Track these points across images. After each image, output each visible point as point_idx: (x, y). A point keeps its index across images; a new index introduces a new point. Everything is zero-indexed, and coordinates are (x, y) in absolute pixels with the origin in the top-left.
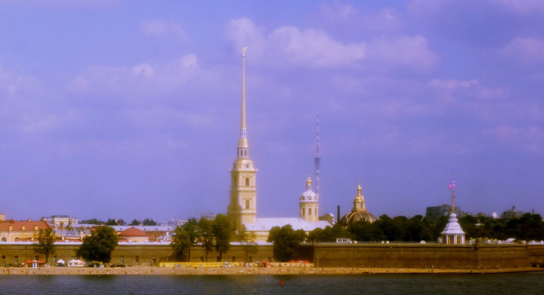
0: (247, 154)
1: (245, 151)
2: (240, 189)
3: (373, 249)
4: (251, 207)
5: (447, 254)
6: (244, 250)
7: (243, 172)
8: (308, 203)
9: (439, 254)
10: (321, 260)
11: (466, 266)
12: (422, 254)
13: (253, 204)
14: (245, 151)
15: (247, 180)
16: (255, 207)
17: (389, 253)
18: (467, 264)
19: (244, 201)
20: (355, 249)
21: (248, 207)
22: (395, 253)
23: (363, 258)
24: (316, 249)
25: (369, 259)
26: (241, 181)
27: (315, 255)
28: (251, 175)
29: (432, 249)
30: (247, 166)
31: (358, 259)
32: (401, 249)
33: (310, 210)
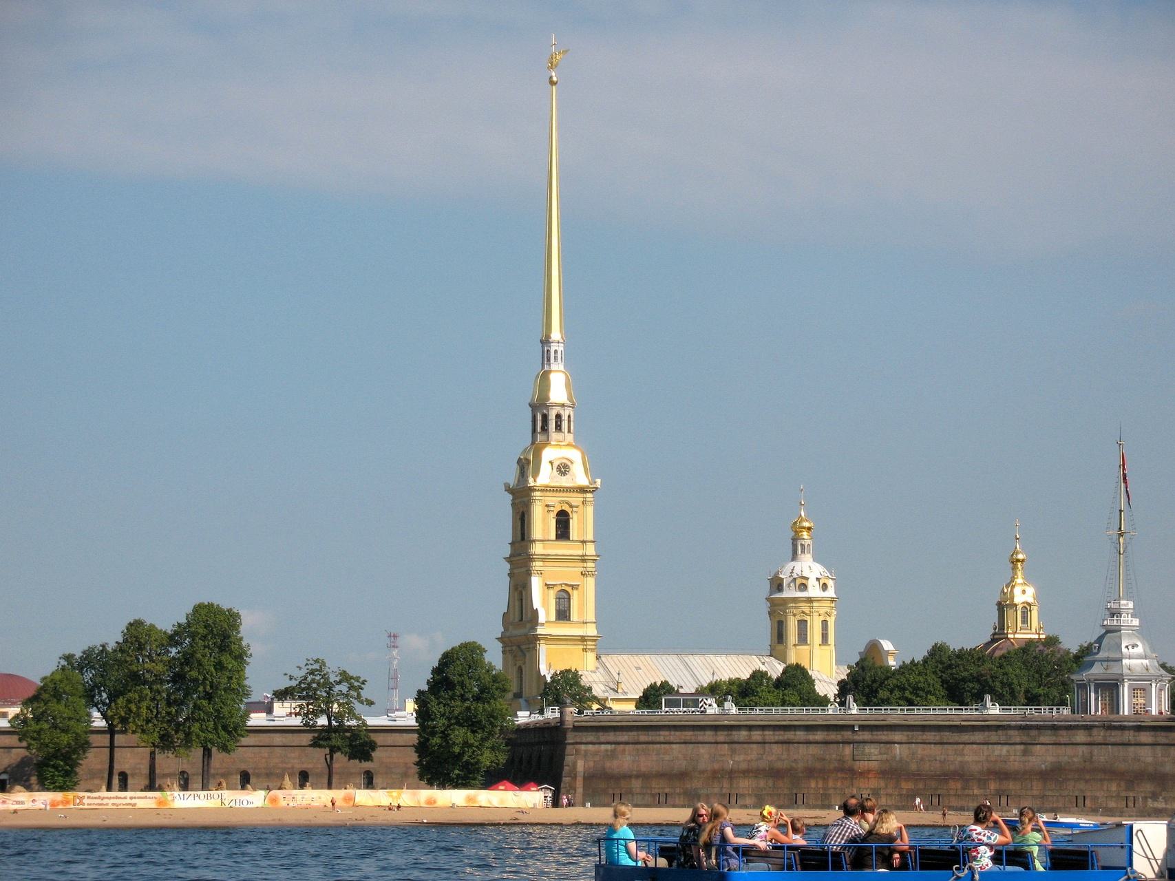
0: (565, 425)
1: (558, 416)
2: (537, 549)
3: (790, 735)
4: (574, 616)
5: (1073, 756)
6: (315, 744)
7: (546, 489)
8: (795, 600)
9: (1043, 756)
10: (589, 778)
11: (1150, 803)
12: (973, 756)
13: (585, 604)
14: (558, 416)
15: (563, 522)
16: (591, 617)
17: (848, 750)
18: (1154, 797)
19: (552, 594)
20: (722, 736)
21: (563, 614)
22: (872, 750)
23: (746, 773)
24: (571, 737)
25: (775, 774)
26: (542, 524)
27: (569, 759)
28: (576, 499)
29: (1016, 736)
30: (563, 469)
31: (731, 774)
32: (897, 736)
33: (802, 624)
